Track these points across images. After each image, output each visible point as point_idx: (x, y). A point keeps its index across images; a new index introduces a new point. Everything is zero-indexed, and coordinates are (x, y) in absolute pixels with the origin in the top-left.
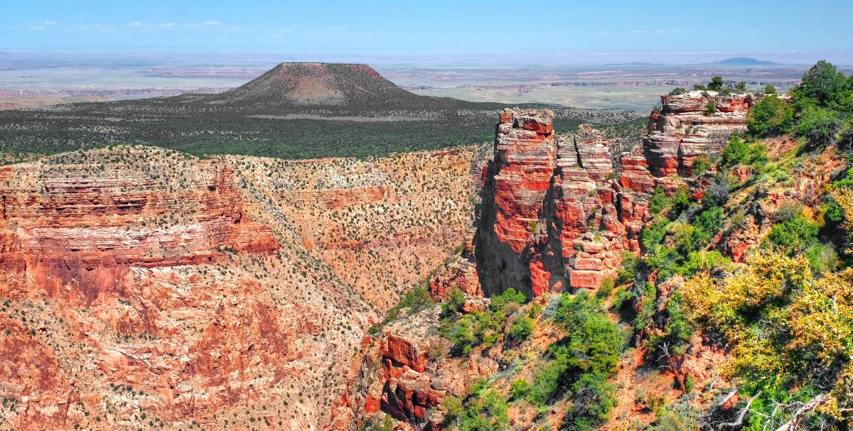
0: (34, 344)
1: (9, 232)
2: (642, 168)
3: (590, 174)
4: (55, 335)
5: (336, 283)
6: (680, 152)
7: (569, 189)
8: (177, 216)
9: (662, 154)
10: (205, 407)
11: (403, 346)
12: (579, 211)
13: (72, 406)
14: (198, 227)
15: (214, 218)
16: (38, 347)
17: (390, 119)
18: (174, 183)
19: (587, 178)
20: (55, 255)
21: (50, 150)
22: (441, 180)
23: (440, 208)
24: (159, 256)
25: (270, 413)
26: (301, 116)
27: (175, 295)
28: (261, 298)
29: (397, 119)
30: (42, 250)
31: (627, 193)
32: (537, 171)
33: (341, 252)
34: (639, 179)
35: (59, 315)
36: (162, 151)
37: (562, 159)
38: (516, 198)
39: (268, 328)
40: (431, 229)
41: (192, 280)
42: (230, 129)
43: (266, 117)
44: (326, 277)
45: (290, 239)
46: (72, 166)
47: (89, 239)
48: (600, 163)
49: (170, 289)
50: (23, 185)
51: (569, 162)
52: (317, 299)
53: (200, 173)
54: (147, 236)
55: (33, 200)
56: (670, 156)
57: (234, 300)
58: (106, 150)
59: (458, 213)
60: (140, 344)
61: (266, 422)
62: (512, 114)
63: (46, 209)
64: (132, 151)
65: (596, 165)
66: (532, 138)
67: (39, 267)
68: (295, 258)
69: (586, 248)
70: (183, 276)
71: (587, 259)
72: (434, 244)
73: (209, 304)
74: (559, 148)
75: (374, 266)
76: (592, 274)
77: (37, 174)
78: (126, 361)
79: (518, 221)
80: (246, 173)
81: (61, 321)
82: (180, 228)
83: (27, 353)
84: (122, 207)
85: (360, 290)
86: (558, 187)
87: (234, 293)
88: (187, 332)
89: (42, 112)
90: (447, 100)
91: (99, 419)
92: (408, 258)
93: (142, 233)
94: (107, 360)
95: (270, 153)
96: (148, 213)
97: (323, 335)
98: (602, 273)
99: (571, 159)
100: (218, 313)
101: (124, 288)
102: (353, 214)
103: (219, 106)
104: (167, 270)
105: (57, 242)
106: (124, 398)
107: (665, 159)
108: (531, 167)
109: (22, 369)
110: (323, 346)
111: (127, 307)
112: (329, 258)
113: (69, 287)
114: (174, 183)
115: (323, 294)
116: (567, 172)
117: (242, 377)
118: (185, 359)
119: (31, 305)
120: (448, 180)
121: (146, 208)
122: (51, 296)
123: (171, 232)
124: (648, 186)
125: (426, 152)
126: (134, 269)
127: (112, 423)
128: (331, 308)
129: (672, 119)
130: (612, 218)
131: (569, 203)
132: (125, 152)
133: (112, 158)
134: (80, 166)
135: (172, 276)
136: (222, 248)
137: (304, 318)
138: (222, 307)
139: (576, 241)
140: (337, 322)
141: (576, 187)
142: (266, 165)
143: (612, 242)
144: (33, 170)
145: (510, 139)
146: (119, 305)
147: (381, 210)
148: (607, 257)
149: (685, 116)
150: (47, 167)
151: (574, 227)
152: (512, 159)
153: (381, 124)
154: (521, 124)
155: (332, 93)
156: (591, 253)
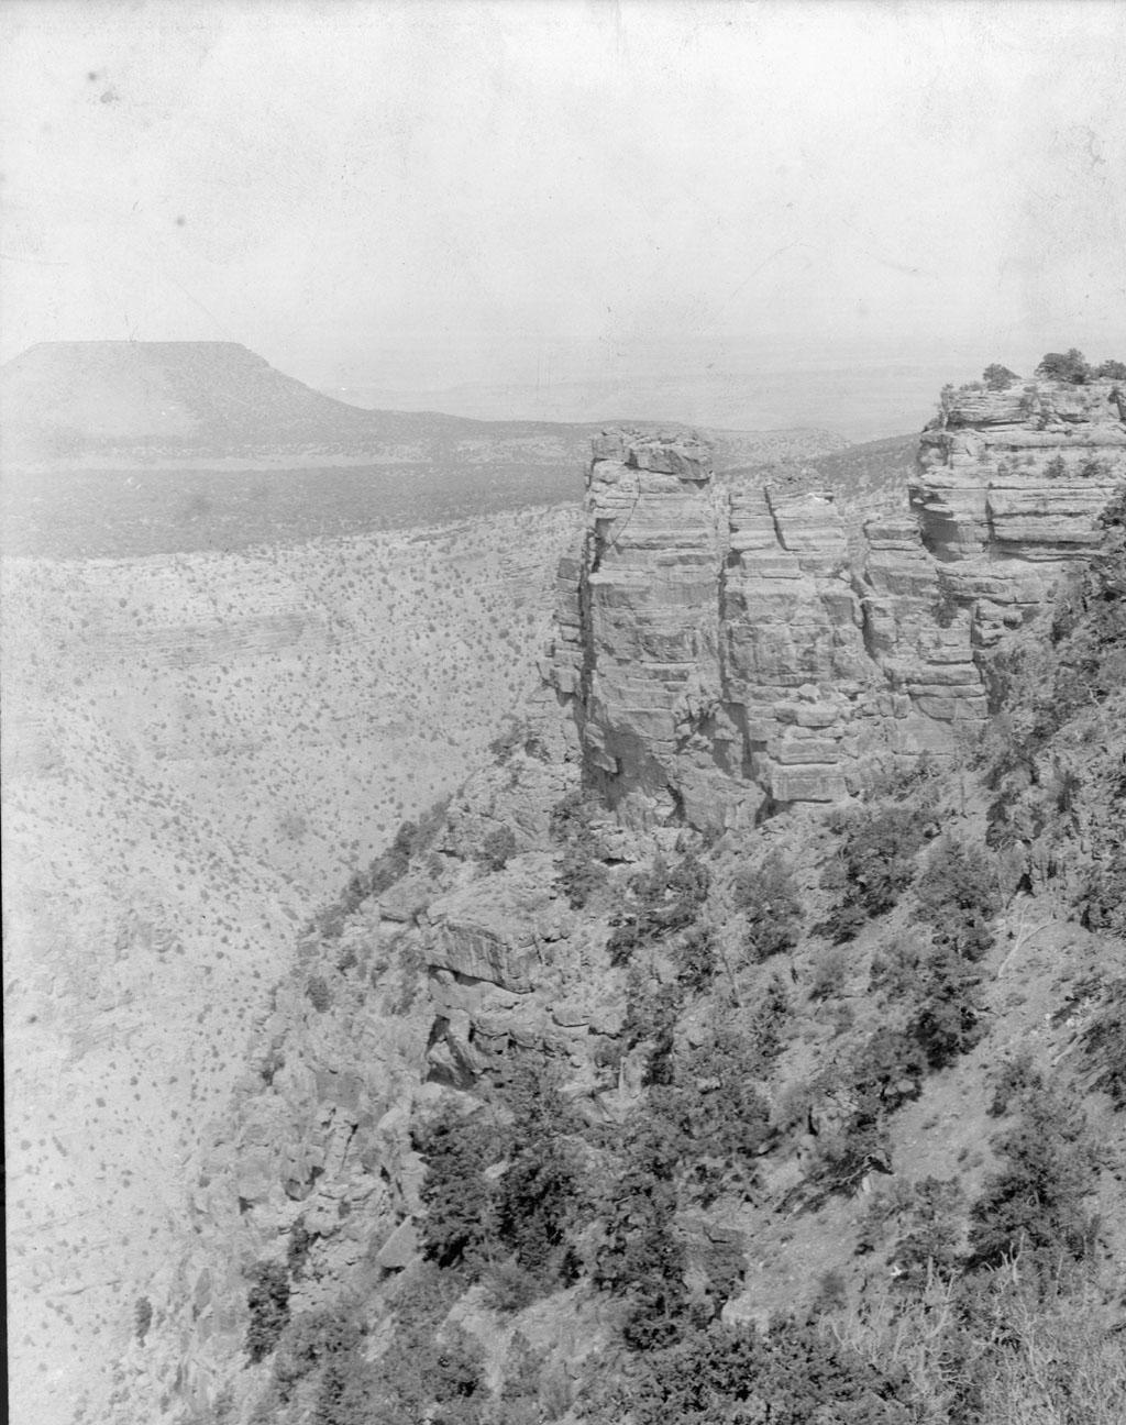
2: (909, 544)
3: (801, 562)
6: (989, 510)
7: (761, 596)
9: (951, 514)
11: (479, 941)
12: (782, 643)
19: (796, 571)
31: (878, 597)
32: (684, 560)
34: (906, 569)
37: (739, 533)
38: (640, 621)
48: (822, 537)
51: (757, 538)
56: (968, 517)
61: (59, 1147)
62: (622, 441)
65: (813, 542)
66: (670, 490)
69: (802, 718)
71: (808, 741)
72: (422, 736)
74: (734, 508)
76: (817, 772)
79: (646, 670)
86: (734, 594)
98: (837, 767)
99: (760, 533)
107: (955, 524)
108: (670, 553)
116: (754, 561)
124: (924, 582)
129: (967, 440)
130: (854, 652)
131: (760, 626)
137: (133, 915)
139: (783, 704)
141: (774, 591)
143: (857, 703)
145: (621, 494)
148: (847, 734)
149: (994, 434)
151: (772, 675)
152: (626, 537)
154: (643, 461)
156: (814, 728)
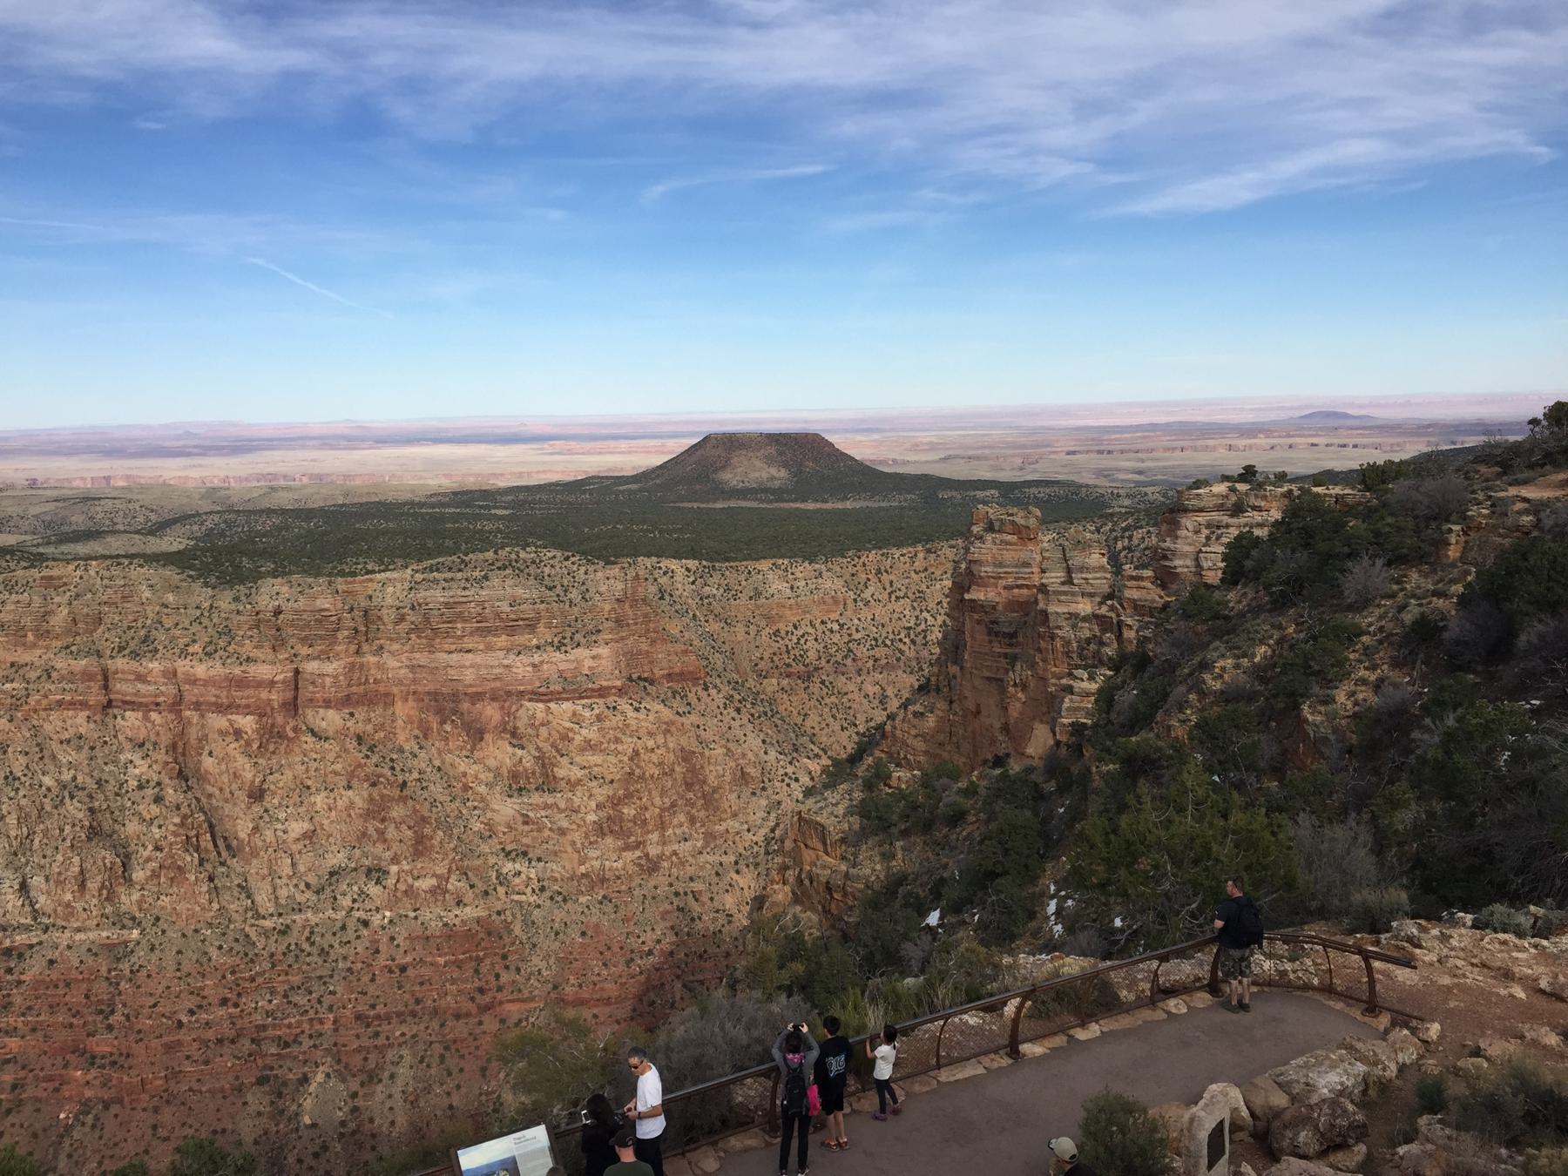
0: (403, 799)
1: (373, 659)
4: (432, 787)
5: (779, 722)
8: (578, 637)
10: (618, 878)
13: (453, 878)
14: (604, 651)
15: (622, 639)
16: (410, 803)
17: (849, 505)
18: (574, 594)
20: (431, 687)
21: (422, 553)
22: (914, 588)
23: (912, 624)
24: (558, 688)
25: (697, 886)
26: (733, 503)
27: (577, 737)
28: (684, 742)
29: (858, 505)
30: (414, 681)
33: (785, 682)
35: (437, 763)
36: (559, 554)
39: (694, 779)
40: (901, 651)
41: (599, 718)
42: (644, 522)
43: (690, 505)
44: (767, 713)
45: (719, 664)
46: (449, 575)
47: (472, 666)
49: (571, 730)
50: (389, 601)
52: (754, 741)
53: (607, 582)
54: (542, 662)
55: (402, 619)
57: (651, 744)
58: (490, 555)
59: (936, 629)
60: (536, 798)
63: (416, 629)
64: (523, 555)
67: (411, 703)
68: (726, 689)
70: (587, 713)
73: (620, 748)
75: (827, 700)
77: (407, 585)
78: (520, 819)
80: (663, 580)
81: (439, 769)
82: (581, 653)
83: (397, 812)
84: (511, 630)
85: (809, 730)
87: (651, 734)
88: (594, 783)
89: (412, 504)
90: (925, 478)
91: (486, 893)
92: (870, 689)
93: (537, 658)
94: (497, 818)
95: (693, 554)
96: (544, 633)
97: (764, 789)
100: (631, 759)
101: (516, 728)
102: (800, 633)
103: (631, 492)
104: (567, 705)
105: (433, 671)
106: (517, 866)
109: (391, 832)
110: (764, 802)
111: (520, 752)
112: (769, 690)
113: (448, 727)
114: (574, 594)
115: (762, 736)
117: (664, 842)
118: (592, 817)
119: (401, 750)
120: (923, 587)
121: (541, 629)
122: (426, 737)
123: (572, 657)
125: (894, 550)
126: (528, 704)
127: (503, 897)
128: (773, 754)
132: (513, 556)
133: (499, 564)
134: (459, 575)
135: (574, 714)
136: (635, 676)
138: (636, 753)
140: (781, 771)
142: (688, 570)
144: (402, 581)
146: (510, 749)
147: (836, 627)
150: (419, 577)
153: (834, 512)
155: (773, 471)
